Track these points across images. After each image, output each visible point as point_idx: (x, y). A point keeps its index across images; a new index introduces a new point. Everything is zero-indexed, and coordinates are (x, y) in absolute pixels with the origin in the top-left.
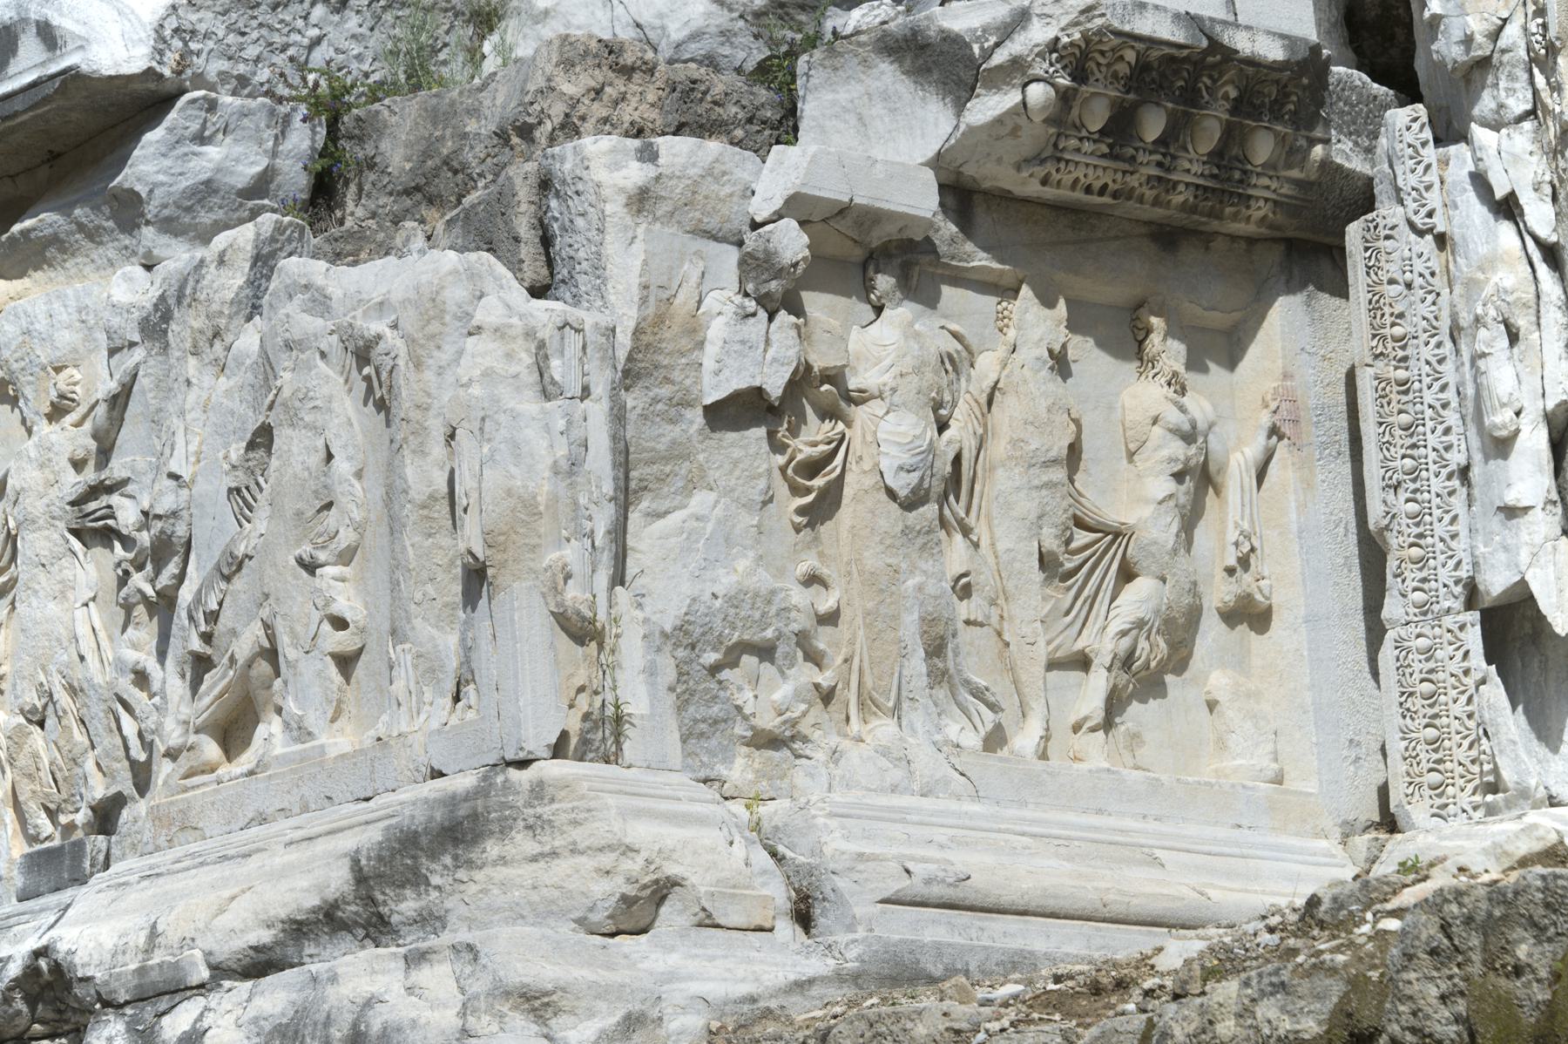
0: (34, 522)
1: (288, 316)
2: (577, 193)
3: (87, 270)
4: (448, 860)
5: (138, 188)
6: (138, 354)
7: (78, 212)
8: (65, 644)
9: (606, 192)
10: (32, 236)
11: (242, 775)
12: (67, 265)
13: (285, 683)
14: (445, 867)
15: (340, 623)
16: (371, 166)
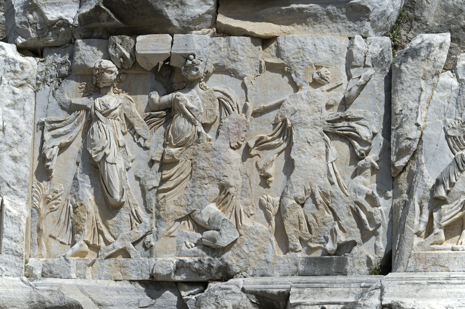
0: (305, 124)
3: (325, 30)
5: (369, 6)
6: (370, 71)
7: (329, 7)
8: (323, 176)
10: (305, 11)
12: (316, 26)
16: (417, 19)
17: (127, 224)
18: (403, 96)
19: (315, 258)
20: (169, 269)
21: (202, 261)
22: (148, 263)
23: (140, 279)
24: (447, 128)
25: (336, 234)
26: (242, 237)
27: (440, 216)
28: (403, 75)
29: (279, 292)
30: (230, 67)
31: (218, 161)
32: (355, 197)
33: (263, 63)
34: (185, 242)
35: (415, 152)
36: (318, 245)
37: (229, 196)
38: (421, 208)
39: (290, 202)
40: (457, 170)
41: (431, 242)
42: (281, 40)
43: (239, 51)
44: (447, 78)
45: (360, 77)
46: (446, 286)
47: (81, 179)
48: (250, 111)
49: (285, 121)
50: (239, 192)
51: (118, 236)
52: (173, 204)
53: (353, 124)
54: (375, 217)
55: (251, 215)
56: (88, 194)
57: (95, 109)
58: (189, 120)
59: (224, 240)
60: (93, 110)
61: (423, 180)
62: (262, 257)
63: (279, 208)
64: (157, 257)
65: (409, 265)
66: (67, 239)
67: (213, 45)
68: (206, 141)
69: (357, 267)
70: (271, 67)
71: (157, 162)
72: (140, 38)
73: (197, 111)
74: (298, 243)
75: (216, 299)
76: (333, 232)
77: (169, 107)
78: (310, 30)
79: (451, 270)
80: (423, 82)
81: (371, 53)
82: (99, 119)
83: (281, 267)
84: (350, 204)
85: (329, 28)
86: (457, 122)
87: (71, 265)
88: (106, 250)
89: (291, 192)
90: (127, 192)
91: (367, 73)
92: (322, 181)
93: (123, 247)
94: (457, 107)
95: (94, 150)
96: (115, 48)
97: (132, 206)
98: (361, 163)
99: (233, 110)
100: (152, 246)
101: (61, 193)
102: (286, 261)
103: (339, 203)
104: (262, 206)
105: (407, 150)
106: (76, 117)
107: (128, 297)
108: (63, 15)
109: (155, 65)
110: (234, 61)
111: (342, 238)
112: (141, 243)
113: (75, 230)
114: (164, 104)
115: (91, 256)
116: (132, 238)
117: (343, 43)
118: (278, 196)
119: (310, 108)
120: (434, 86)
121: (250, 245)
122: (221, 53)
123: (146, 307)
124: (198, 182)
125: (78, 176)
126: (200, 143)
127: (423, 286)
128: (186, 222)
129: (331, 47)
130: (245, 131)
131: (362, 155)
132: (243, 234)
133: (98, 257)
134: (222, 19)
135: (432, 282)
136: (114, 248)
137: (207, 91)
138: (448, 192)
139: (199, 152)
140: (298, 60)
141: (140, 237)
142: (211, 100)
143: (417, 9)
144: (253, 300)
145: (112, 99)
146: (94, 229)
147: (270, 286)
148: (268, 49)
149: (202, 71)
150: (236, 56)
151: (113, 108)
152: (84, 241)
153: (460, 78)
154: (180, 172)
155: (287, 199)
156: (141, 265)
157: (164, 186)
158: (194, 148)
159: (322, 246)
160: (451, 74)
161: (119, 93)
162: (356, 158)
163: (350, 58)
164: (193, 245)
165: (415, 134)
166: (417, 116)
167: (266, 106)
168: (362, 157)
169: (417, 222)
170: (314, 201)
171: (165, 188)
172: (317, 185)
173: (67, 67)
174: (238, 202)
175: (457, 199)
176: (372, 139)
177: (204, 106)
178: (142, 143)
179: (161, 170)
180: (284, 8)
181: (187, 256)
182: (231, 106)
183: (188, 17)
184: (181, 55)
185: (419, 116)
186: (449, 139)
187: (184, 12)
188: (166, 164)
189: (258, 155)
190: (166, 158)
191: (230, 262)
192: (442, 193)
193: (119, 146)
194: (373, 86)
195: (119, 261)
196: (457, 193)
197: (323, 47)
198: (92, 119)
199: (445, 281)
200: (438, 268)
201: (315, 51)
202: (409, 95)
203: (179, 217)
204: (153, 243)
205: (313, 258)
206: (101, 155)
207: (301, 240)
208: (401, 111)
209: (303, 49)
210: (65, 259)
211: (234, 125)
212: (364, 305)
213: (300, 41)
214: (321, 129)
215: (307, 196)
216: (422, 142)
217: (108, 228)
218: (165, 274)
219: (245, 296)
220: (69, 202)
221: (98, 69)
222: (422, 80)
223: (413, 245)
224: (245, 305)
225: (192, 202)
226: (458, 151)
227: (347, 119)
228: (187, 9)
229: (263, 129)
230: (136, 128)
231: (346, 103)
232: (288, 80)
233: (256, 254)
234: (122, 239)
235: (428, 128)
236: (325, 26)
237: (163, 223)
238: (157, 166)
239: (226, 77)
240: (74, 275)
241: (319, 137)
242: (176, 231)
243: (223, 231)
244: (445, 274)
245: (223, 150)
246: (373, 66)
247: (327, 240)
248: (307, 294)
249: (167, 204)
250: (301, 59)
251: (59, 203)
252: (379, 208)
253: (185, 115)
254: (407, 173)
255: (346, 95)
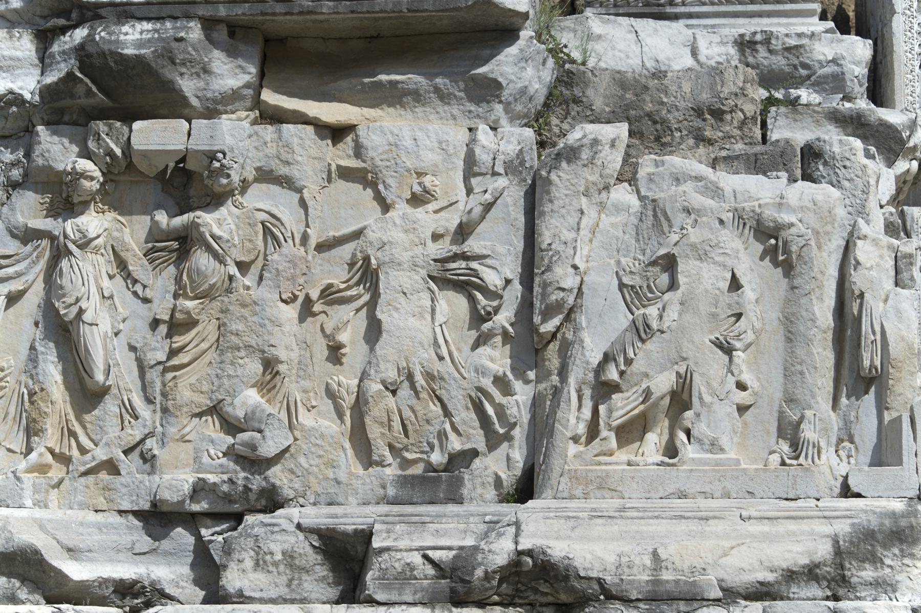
0: (399, 264)
1: (685, 192)
2: (845, 167)
3: (432, 117)
4: (896, 551)
5: (500, 79)
6: (502, 182)
7: (439, 80)
8: (426, 347)
9: (870, 172)
10: (400, 86)
11: (653, 464)
12: (417, 110)
13: (698, 415)
14: (895, 555)
15: (741, 386)
16: (576, 101)
17: (114, 421)
18: (553, 221)
19: (414, 477)
20: (181, 493)
21: (235, 480)
22: (147, 484)
23: (136, 508)
24: (621, 273)
25: (447, 439)
26: (297, 442)
27: (610, 411)
28: (553, 189)
29: (356, 530)
30: (281, 173)
31: (261, 321)
32: (476, 380)
33: (334, 167)
34: (207, 450)
35: (571, 310)
36: (418, 455)
37: (278, 377)
38: (580, 398)
39: (375, 387)
40: (636, 338)
41: (596, 452)
42: (362, 131)
43: (296, 148)
44: (622, 194)
45: (486, 191)
46: (619, 521)
47: (43, 349)
48: (313, 242)
49: (367, 259)
50: (294, 371)
51: (101, 440)
52: (189, 388)
53: (474, 265)
54: (508, 412)
55: (313, 407)
56: (52, 372)
57: (66, 236)
58: (216, 256)
59: (269, 446)
60: (62, 238)
61: (583, 354)
62: (330, 473)
63: (358, 396)
64: (162, 473)
65: (560, 488)
66: (18, 444)
67: (255, 138)
68: (242, 290)
69: (479, 490)
70: (346, 174)
71: (164, 322)
72: (137, 125)
73: (228, 241)
74: (387, 453)
75: (256, 541)
76: (442, 436)
77: (183, 234)
78: (408, 116)
79: (626, 495)
80: (584, 200)
81: (503, 153)
82: (71, 253)
83: (360, 491)
84: (469, 391)
85: (437, 112)
86: (637, 263)
87: (24, 486)
88: (80, 463)
89: (376, 372)
90: (116, 369)
91: (496, 185)
92: (426, 355)
93: (109, 457)
94: (638, 240)
95: (64, 302)
96: (99, 139)
97: (123, 392)
98: (487, 326)
99: (286, 241)
100: (154, 456)
101: (9, 371)
102: (368, 480)
103: (451, 389)
104: (330, 394)
105: (559, 305)
106: (35, 250)
107: (115, 537)
108: (15, 87)
109: (161, 167)
110: (288, 163)
111: (456, 444)
112: (137, 451)
113: (32, 430)
114: (176, 230)
115: (57, 472)
116: (122, 443)
117: (460, 137)
118: (355, 378)
119: (406, 239)
120: (602, 206)
121: (310, 456)
122: (267, 151)
123: (144, 554)
124: (229, 355)
125: (37, 344)
126: (232, 293)
127: (582, 522)
128: (209, 418)
129: (440, 143)
130: (305, 274)
131: (489, 313)
132: (299, 437)
133: (67, 473)
134: (269, 97)
135: (597, 515)
136: (94, 458)
137: (244, 210)
138: (622, 374)
139: (231, 308)
140: (388, 164)
141: (135, 442)
142: (250, 224)
143: (578, 85)
144: (314, 543)
145: (93, 222)
146: (62, 428)
147: (342, 520)
148: (341, 145)
149: (236, 178)
150: (290, 156)
151: (94, 235)
152: (46, 447)
153: (643, 194)
154: (200, 339)
155: (369, 382)
156: (136, 486)
157: (175, 361)
158: (223, 301)
159: (425, 456)
160: (629, 188)
161: (103, 213)
162: (478, 318)
163: (470, 161)
164: (221, 455)
165: (571, 281)
166: (575, 254)
167: (337, 234)
168: (488, 317)
169: (573, 421)
170: (413, 386)
171: (177, 363)
172: (417, 361)
173: (21, 170)
174: (292, 387)
175: (636, 385)
176: (504, 289)
177: (239, 235)
178: (140, 293)
179: (169, 335)
180: (366, 80)
181: (211, 473)
182: (282, 234)
183: (214, 92)
184: (204, 152)
185: (578, 253)
186: (625, 290)
187: (208, 84)
188: (178, 325)
189: (324, 312)
190: (178, 315)
191: (278, 483)
192: (612, 374)
193: (104, 297)
194: (507, 206)
195: (102, 481)
196: (636, 374)
197: (428, 142)
198: (59, 252)
199: (617, 514)
200: (607, 494)
201: (416, 149)
202: (562, 219)
203: (197, 411)
204: (156, 452)
205: (410, 476)
206: (74, 310)
207: (391, 447)
208: (550, 244)
209: (396, 145)
210: (15, 476)
211: (287, 265)
212: (489, 551)
213: (391, 133)
214: (424, 273)
215: (402, 378)
216: (583, 294)
217: (84, 427)
218: (176, 500)
219: (301, 536)
220: (23, 386)
221: (70, 173)
222: (582, 197)
223: (566, 456)
224: (302, 551)
225: (220, 387)
226: (638, 309)
227: (465, 257)
228: (214, 79)
229: (333, 271)
230: (131, 268)
231: (463, 232)
232: (372, 195)
233: (320, 470)
234: (107, 444)
235: (591, 272)
236: (432, 110)
237: (172, 420)
238: (163, 329)
239: (275, 189)
240: (28, 503)
241: (420, 285)
242: (194, 432)
243: (267, 433)
244: (617, 503)
245: (268, 304)
246: (507, 174)
247: (432, 448)
248: (400, 533)
249: (180, 389)
250: (393, 162)
251: (6, 387)
252: (514, 398)
253: (209, 249)
254: (558, 343)
255: (464, 220)
